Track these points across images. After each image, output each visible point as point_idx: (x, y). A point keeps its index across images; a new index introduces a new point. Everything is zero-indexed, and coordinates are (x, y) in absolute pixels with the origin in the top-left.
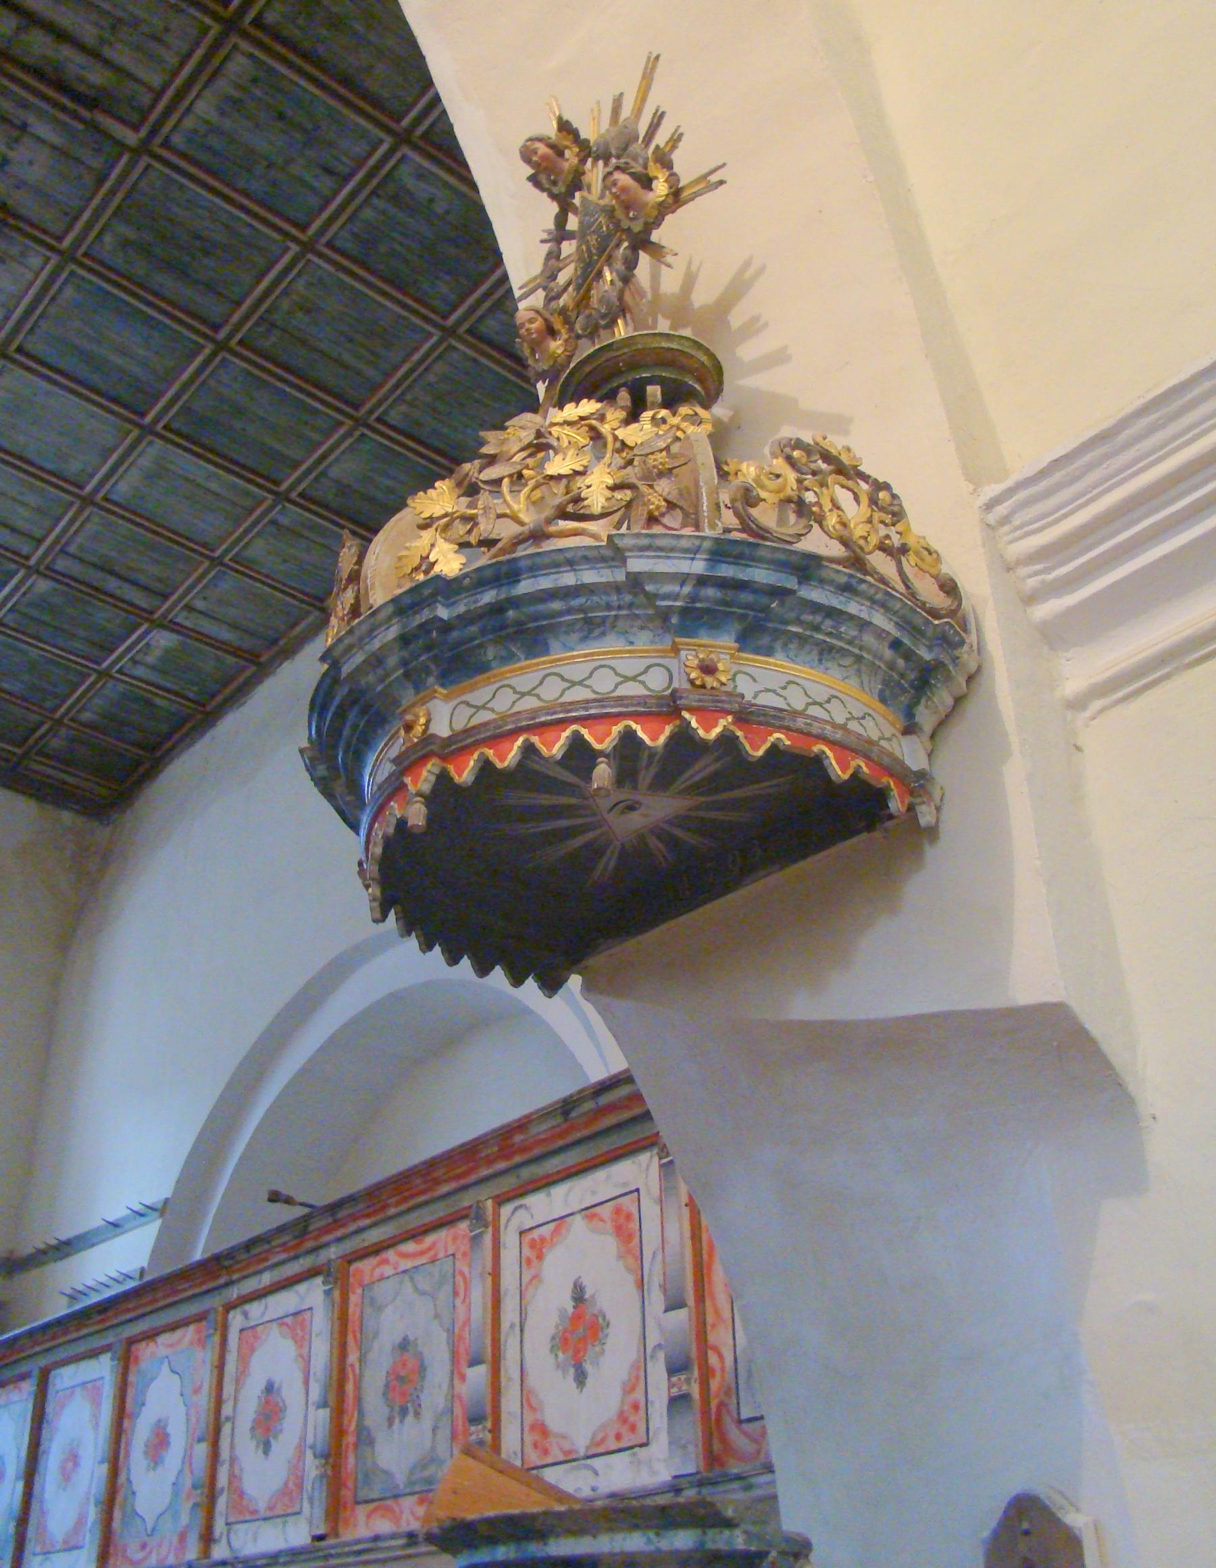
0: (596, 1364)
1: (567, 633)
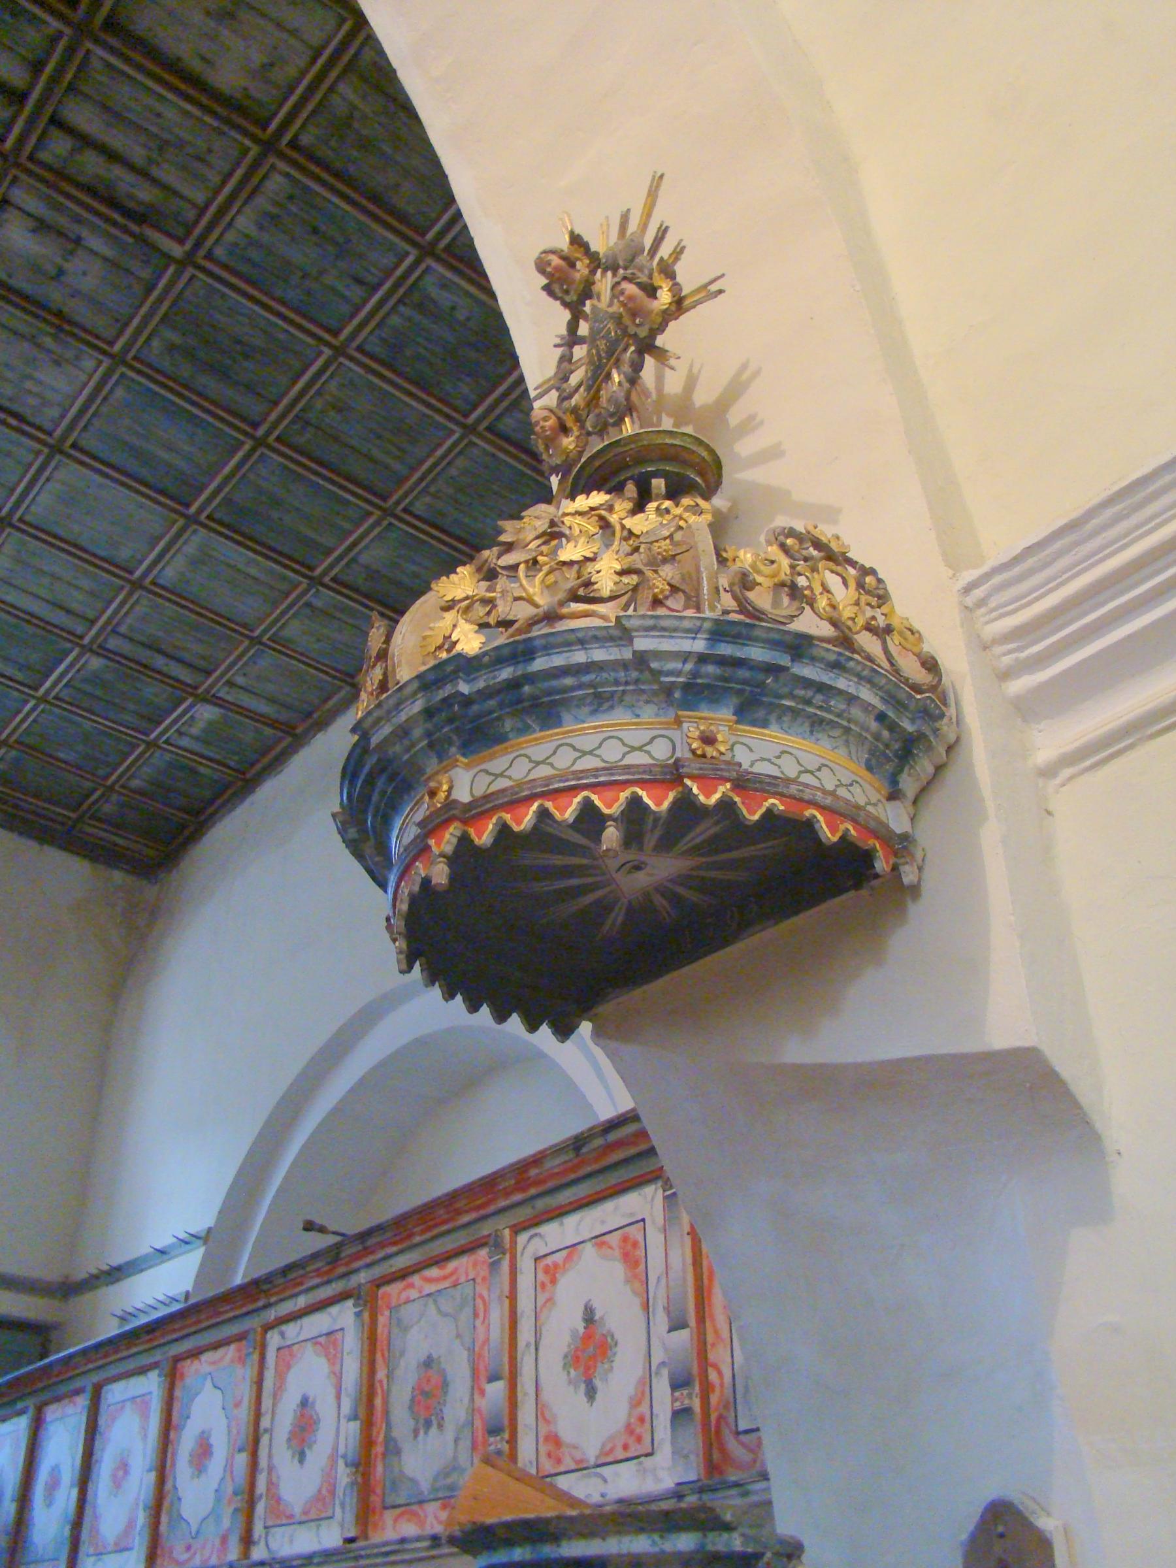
0: (605, 1380)
1: (578, 706)
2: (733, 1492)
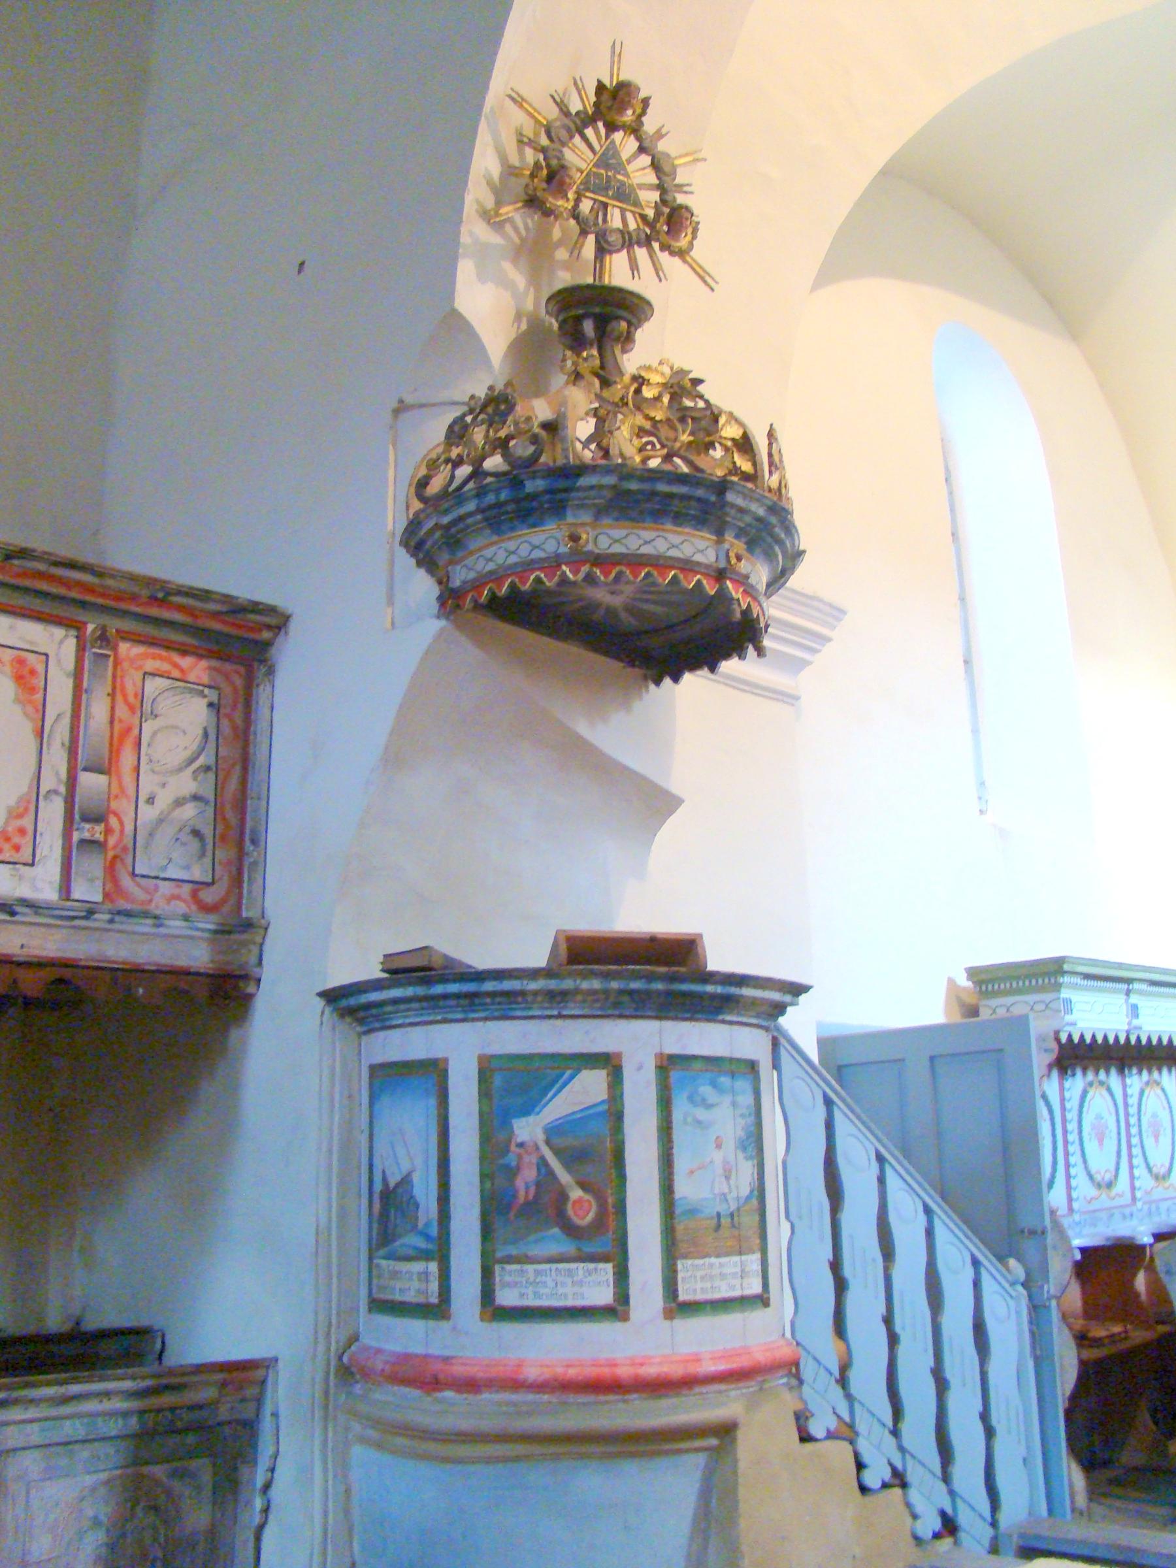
2: (149, 921)
